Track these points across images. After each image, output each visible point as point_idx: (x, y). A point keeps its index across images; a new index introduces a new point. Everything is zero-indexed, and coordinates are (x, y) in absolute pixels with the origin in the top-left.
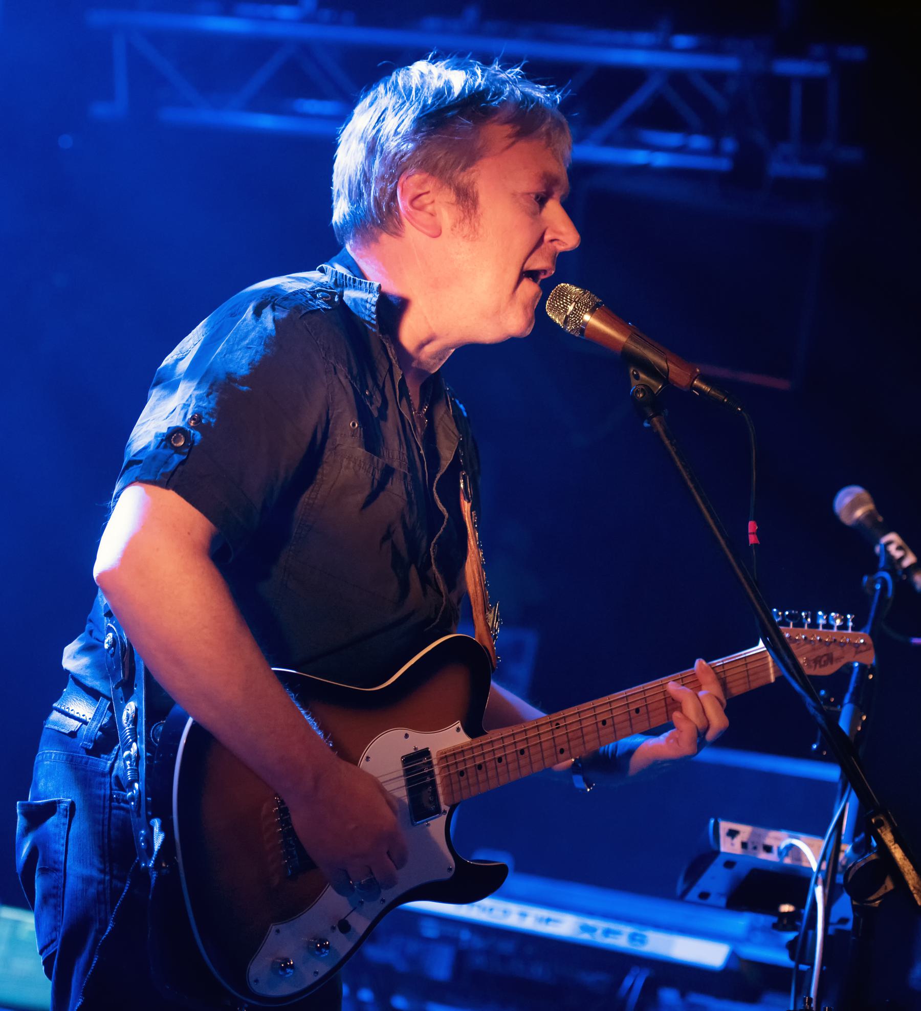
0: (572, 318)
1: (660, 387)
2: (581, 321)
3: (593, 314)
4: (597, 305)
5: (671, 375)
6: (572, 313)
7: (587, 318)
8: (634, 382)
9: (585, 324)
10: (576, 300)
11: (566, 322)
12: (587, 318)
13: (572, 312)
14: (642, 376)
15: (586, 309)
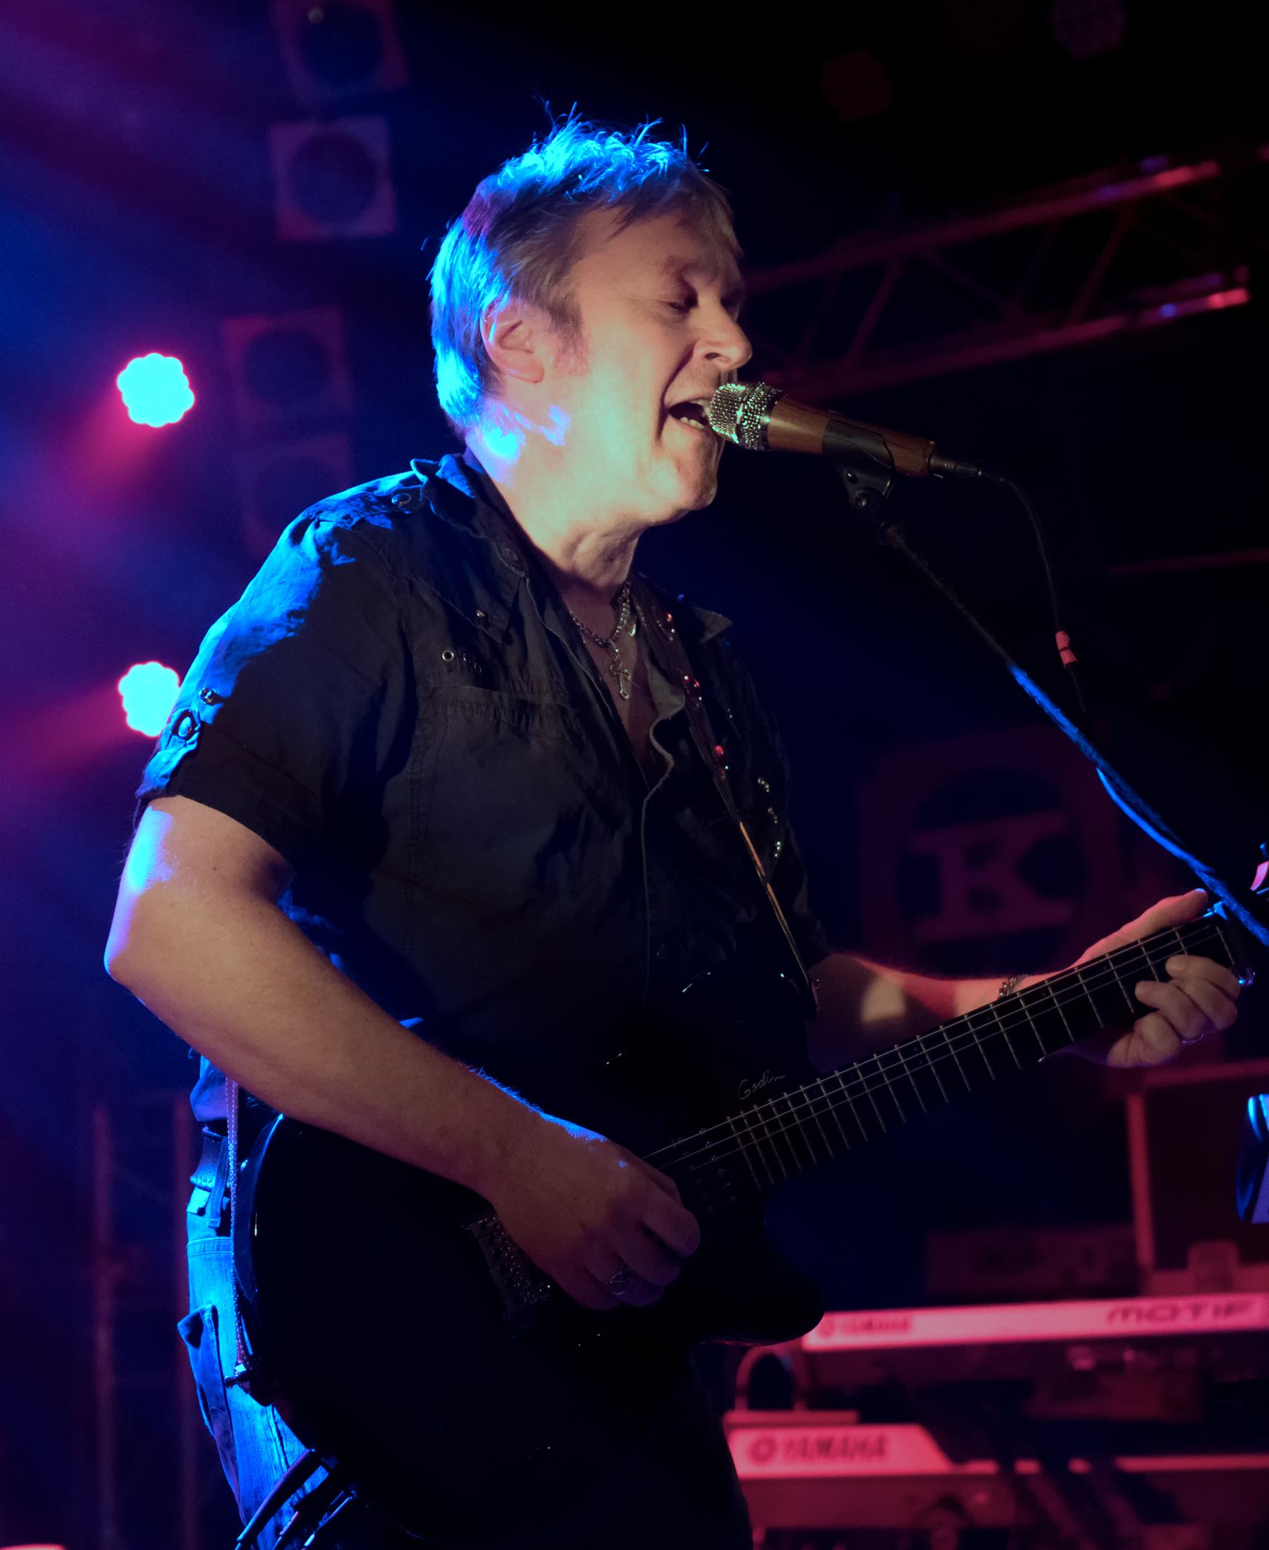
0: (745, 426)
1: (888, 484)
2: (759, 427)
3: (771, 412)
4: (777, 397)
5: (897, 463)
6: (743, 420)
7: (766, 420)
8: (850, 487)
9: (765, 427)
10: (744, 400)
11: (739, 434)
12: (766, 420)
13: (742, 417)
14: (859, 475)
15: (761, 408)
